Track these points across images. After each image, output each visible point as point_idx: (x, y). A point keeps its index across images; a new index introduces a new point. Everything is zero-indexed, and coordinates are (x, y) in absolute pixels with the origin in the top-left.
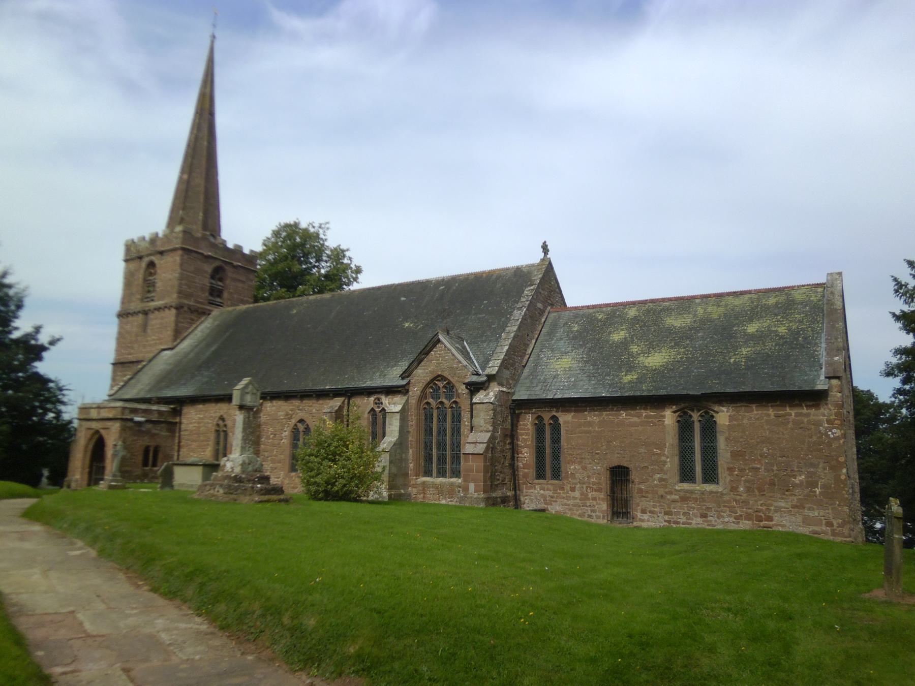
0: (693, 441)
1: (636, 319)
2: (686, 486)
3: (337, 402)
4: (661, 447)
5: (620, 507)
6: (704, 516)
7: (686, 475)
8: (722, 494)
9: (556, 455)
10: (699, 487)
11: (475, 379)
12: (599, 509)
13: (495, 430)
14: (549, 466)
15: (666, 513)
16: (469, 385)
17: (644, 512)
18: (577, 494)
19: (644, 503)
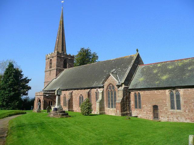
0: (174, 98)
1: (160, 67)
2: (172, 110)
3: (71, 91)
4: (166, 100)
5: (156, 116)
6: (177, 118)
7: (172, 107)
8: (182, 112)
9: (140, 103)
10: (176, 111)
11: (119, 84)
12: (150, 116)
13: (124, 96)
14: (138, 105)
15: (167, 117)
16: (117, 85)
17: (162, 117)
18: (145, 112)
19: (163, 115)
